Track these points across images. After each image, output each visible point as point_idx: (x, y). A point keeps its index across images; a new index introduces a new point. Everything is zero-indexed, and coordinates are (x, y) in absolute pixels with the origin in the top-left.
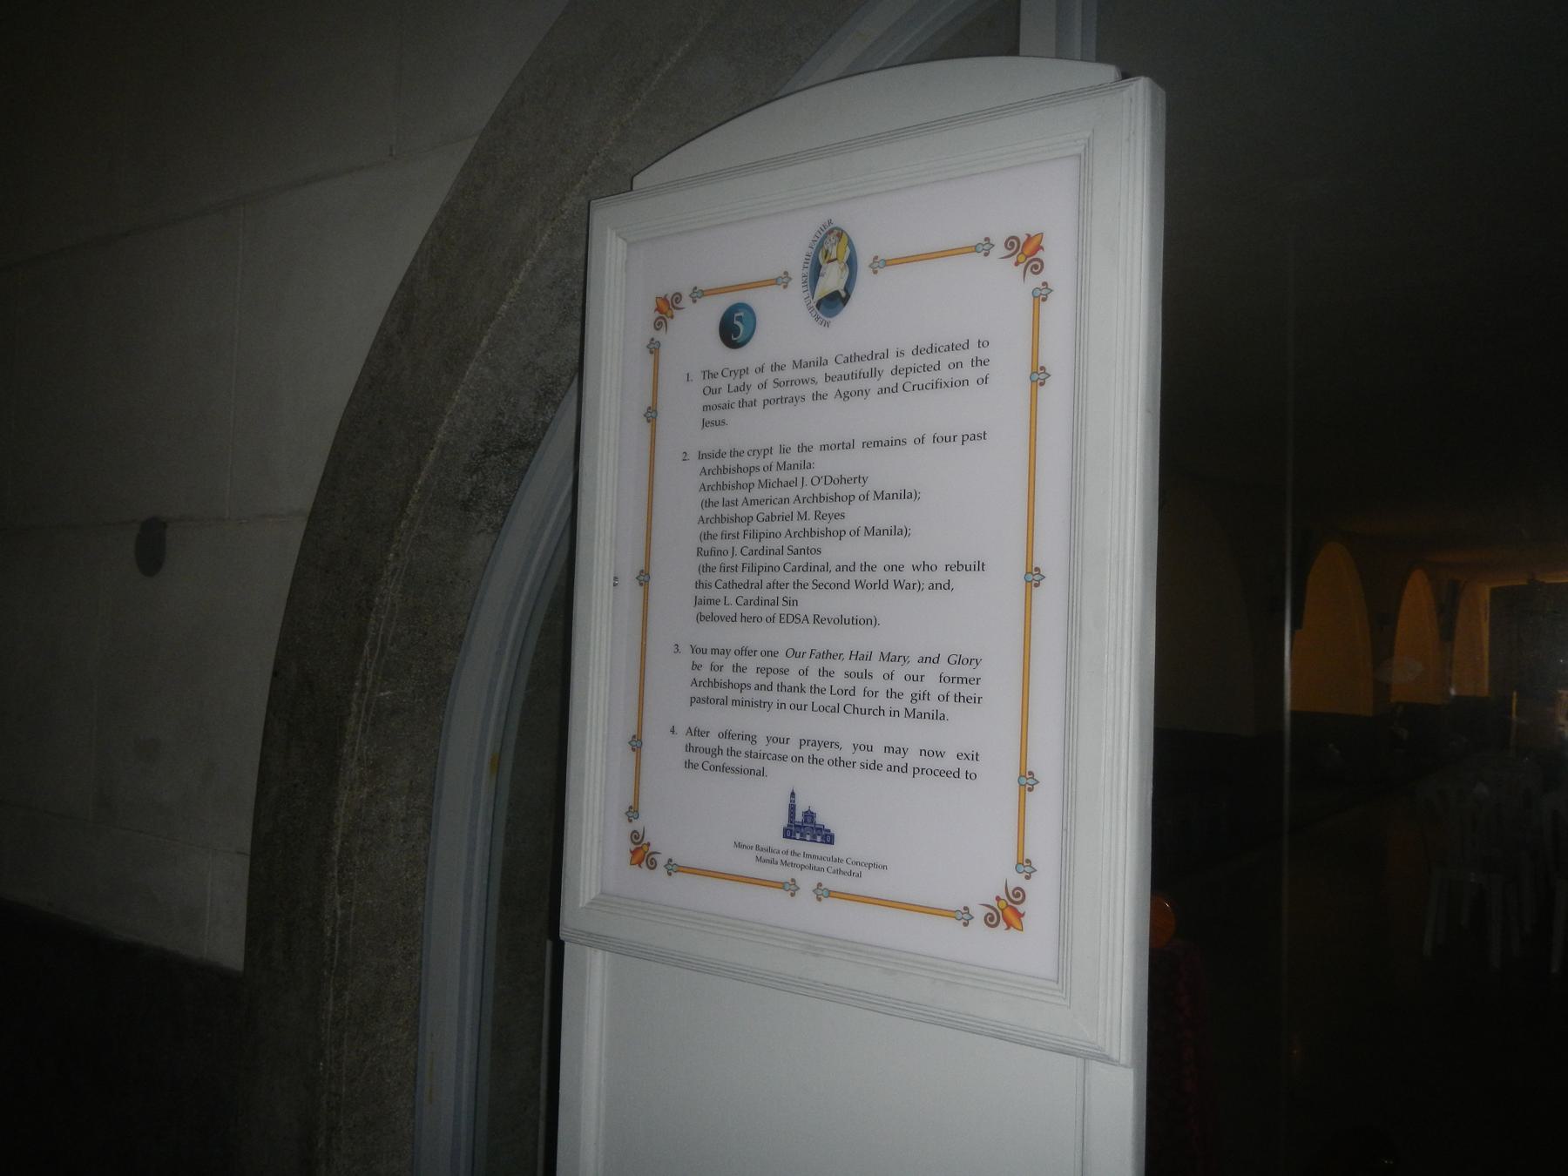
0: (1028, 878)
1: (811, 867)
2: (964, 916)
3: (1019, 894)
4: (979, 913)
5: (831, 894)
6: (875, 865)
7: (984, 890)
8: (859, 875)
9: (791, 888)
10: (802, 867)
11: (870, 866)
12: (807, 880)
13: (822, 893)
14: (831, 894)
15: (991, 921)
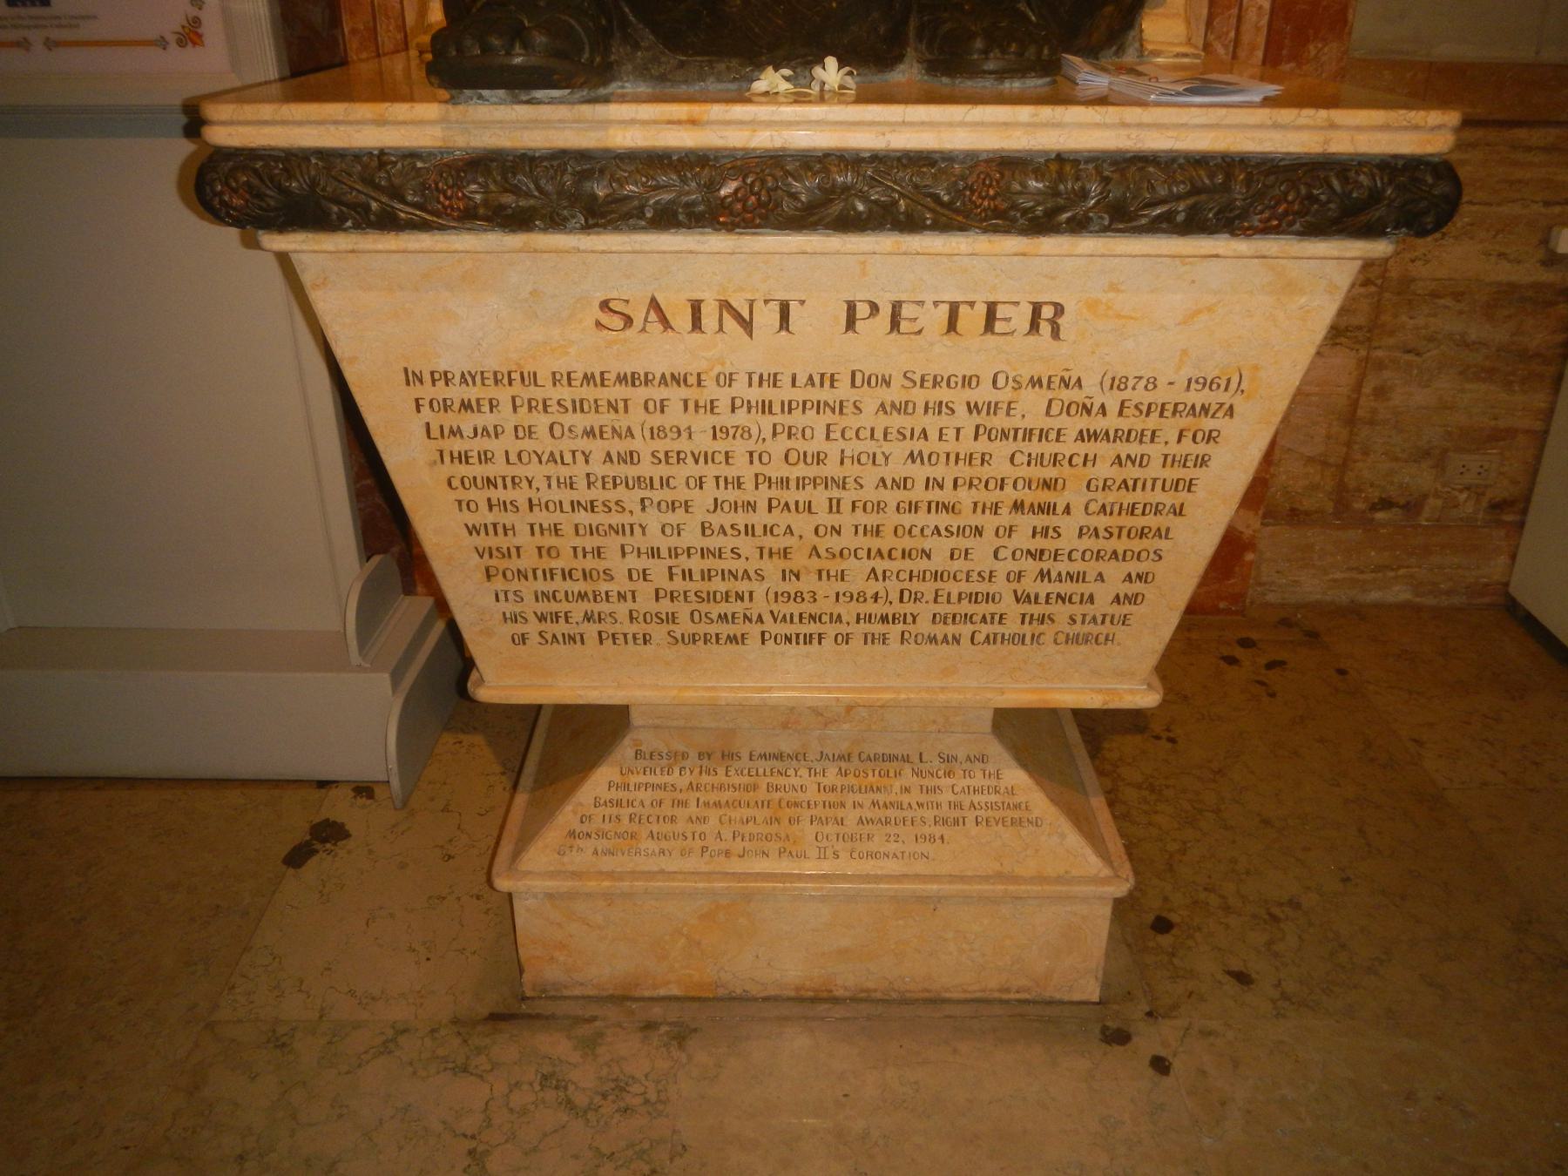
0: (200, 9)
1: (36, 27)
2: (162, 43)
3: (197, 21)
4: (172, 39)
5: (58, 44)
6: (88, 17)
7: (171, 23)
8: (77, 26)
9: (24, 44)
10: (29, 27)
11: (83, 17)
12: (36, 37)
13: (50, 44)
14: (58, 44)
15: (181, 43)
